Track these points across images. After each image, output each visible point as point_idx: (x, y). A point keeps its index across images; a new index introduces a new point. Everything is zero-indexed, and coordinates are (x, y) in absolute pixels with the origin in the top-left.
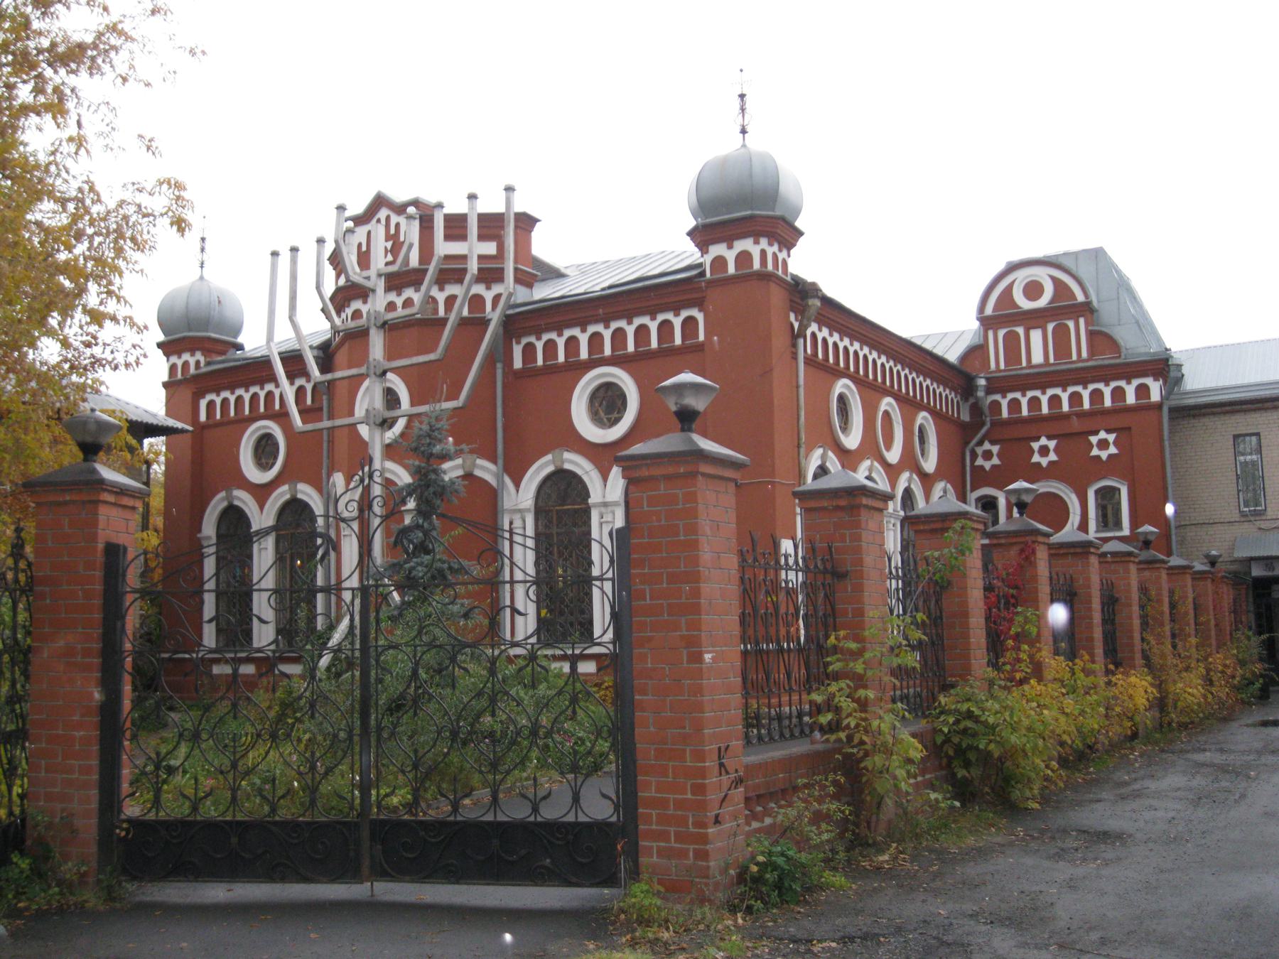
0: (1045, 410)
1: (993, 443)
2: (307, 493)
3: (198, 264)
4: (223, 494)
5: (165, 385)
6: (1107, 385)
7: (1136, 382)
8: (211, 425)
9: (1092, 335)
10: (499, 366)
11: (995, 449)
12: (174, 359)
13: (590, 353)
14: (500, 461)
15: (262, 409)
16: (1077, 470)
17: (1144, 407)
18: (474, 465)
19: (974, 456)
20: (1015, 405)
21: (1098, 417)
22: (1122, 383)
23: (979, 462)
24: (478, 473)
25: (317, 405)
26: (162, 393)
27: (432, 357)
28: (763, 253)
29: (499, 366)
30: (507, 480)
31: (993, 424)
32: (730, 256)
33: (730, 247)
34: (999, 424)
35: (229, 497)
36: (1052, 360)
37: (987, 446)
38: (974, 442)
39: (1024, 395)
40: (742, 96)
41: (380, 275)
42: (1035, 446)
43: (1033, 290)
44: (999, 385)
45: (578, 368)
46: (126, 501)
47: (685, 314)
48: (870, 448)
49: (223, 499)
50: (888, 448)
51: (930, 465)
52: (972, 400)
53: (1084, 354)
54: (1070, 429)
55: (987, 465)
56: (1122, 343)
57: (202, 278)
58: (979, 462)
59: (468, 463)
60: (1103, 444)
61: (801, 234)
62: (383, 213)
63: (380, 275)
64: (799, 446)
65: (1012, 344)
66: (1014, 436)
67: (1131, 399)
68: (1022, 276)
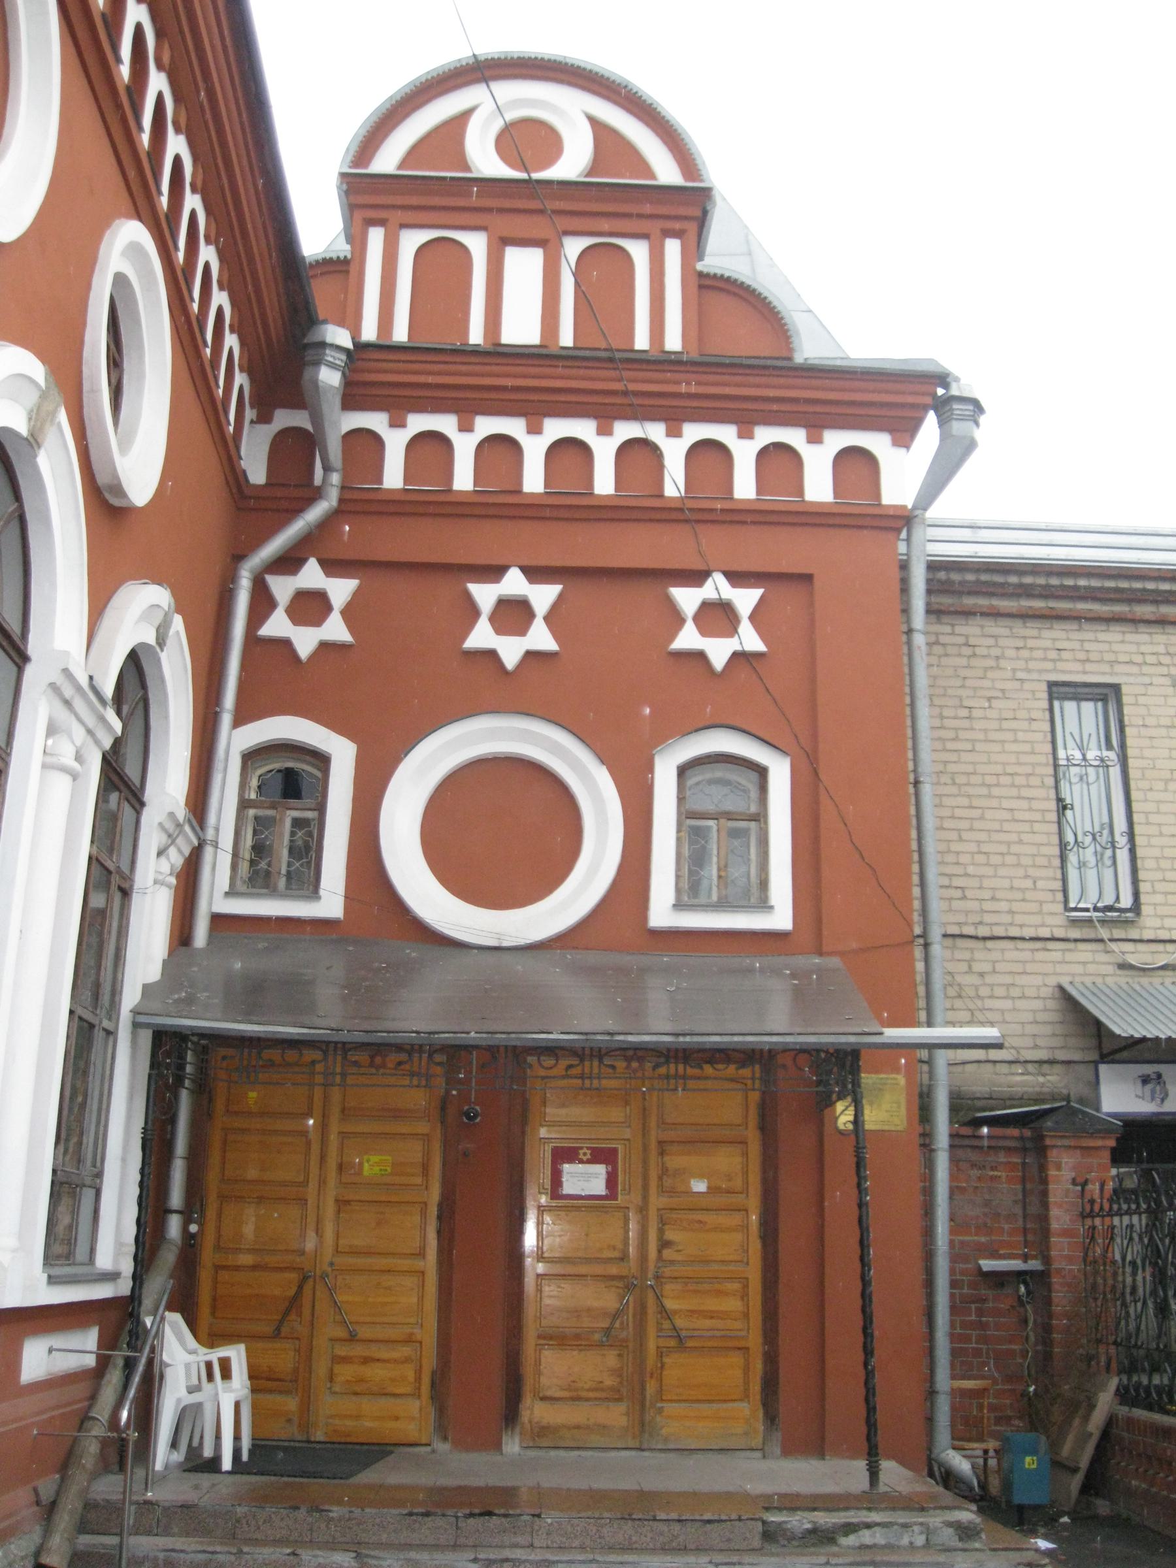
1: (332, 567)
6: (745, 434)
11: (341, 590)
16: (620, 694)
19: (263, 602)
23: (277, 625)
31: (350, 506)
34: (364, 503)
37: (311, 575)
42: (485, 595)
44: (381, 378)
52: (284, 419)
54: (621, 556)
55: (305, 641)
58: (277, 625)
65: (441, 274)
66: (419, 549)
67: (819, 486)
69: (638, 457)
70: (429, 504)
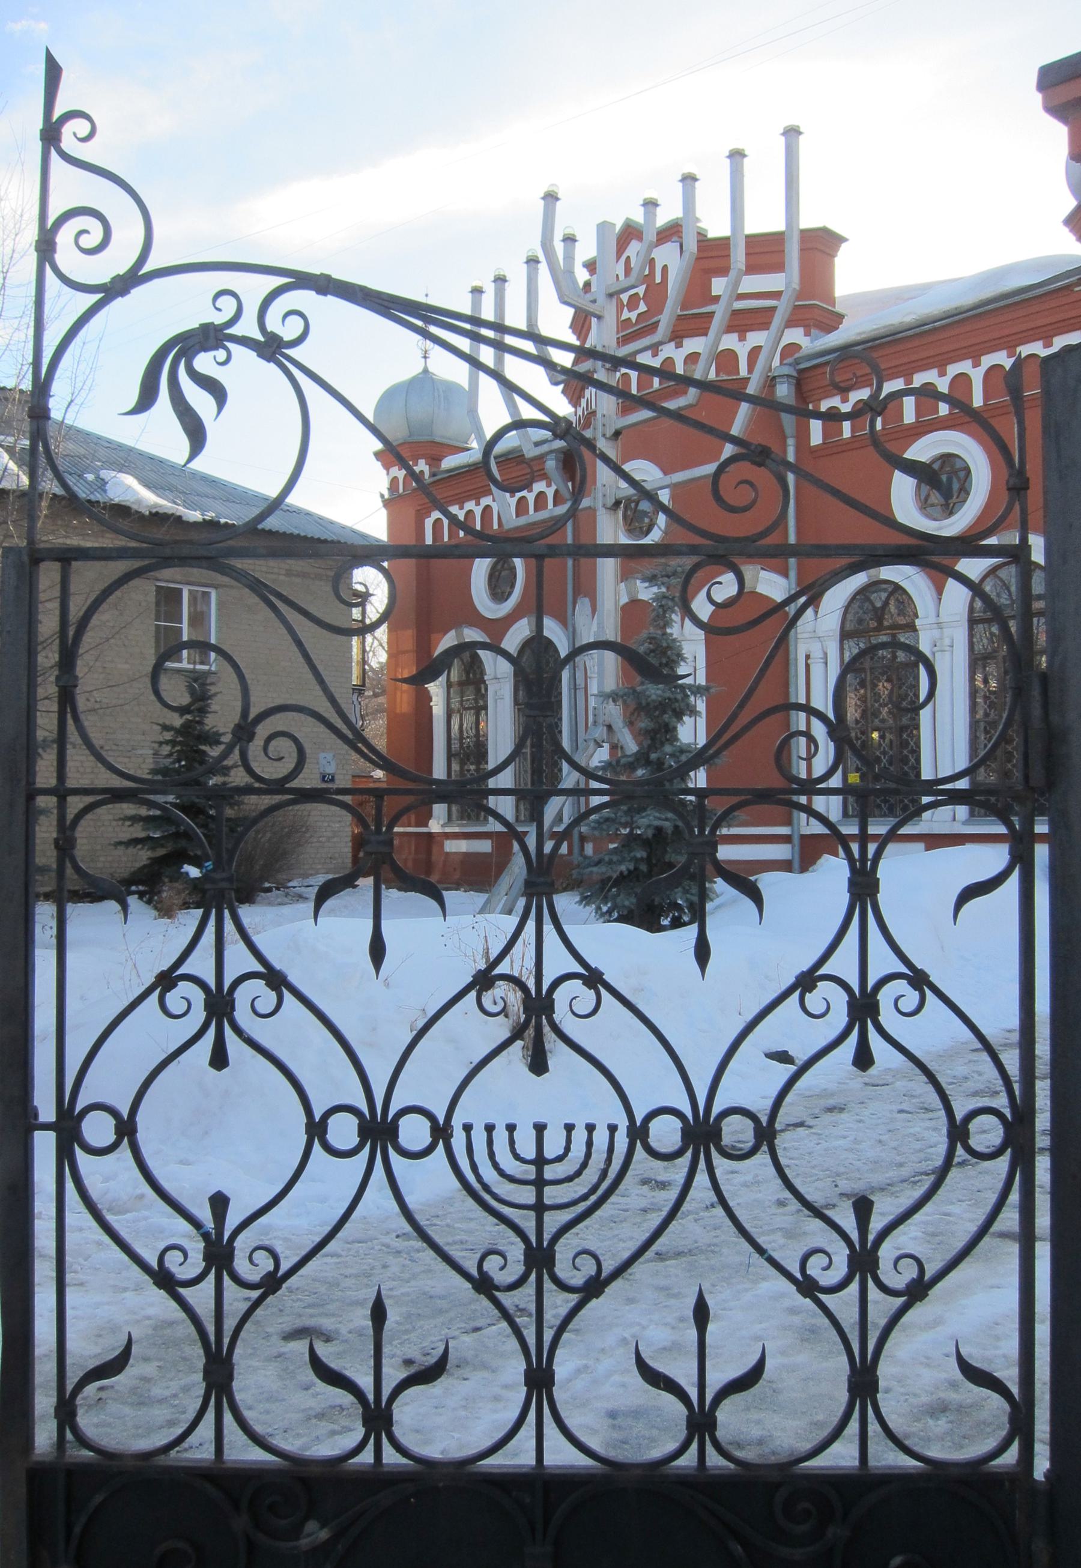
3: (420, 354)
26: (383, 514)
57: (426, 371)
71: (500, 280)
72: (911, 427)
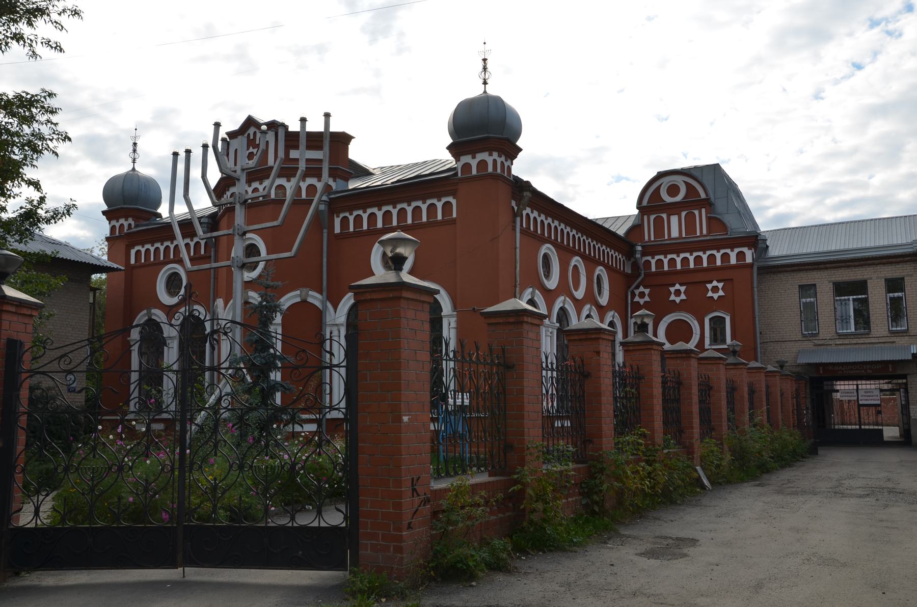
0: (679, 267)
1: (645, 287)
2: (200, 310)
4: (145, 311)
5: (107, 239)
6: (718, 252)
7: (737, 250)
8: (138, 266)
9: (709, 219)
10: (325, 231)
11: (647, 291)
12: (114, 222)
13: (383, 224)
14: (325, 293)
15: (172, 257)
16: (698, 305)
17: (742, 266)
18: (308, 295)
19: (633, 295)
20: (660, 263)
21: (712, 271)
22: (728, 251)
23: (637, 299)
24: (310, 300)
25: (208, 254)
27: (275, 223)
28: (495, 161)
29: (325, 231)
30: (329, 305)
32: (474, 163)
33: (474, 157)
34: (649, 275)
35: (149, 314)
36: (684, 235)
37: (642, 289)
38: (634, 286)
39: (666, 257)
40: (485, 60)
41: (243, 170)
42: (672, 289)
43: (673, 190)
45: (374, 233)
46: (25, 311)
47: (444, 200)
48: (563, 289)
49: (144, 315)
50: (576, 289)
51: (604, 300)
52: (633, 260)
53: (705, 232)
54: (694, 279)
56: (728, 225)
57: (134, 169)
58: (637, 299)
59: (304, 293)
60: (715, 289)
61: (520, 150)
62: (251, 131)
63: (243, 170)
64: (515, 286)
65: (659, 223)
66: (660, 282)
67: (733, 261)
68: (666, 181)
69: (698, 260)
70: (661, 274)
71: (188, 152)
72: (380, 230)
